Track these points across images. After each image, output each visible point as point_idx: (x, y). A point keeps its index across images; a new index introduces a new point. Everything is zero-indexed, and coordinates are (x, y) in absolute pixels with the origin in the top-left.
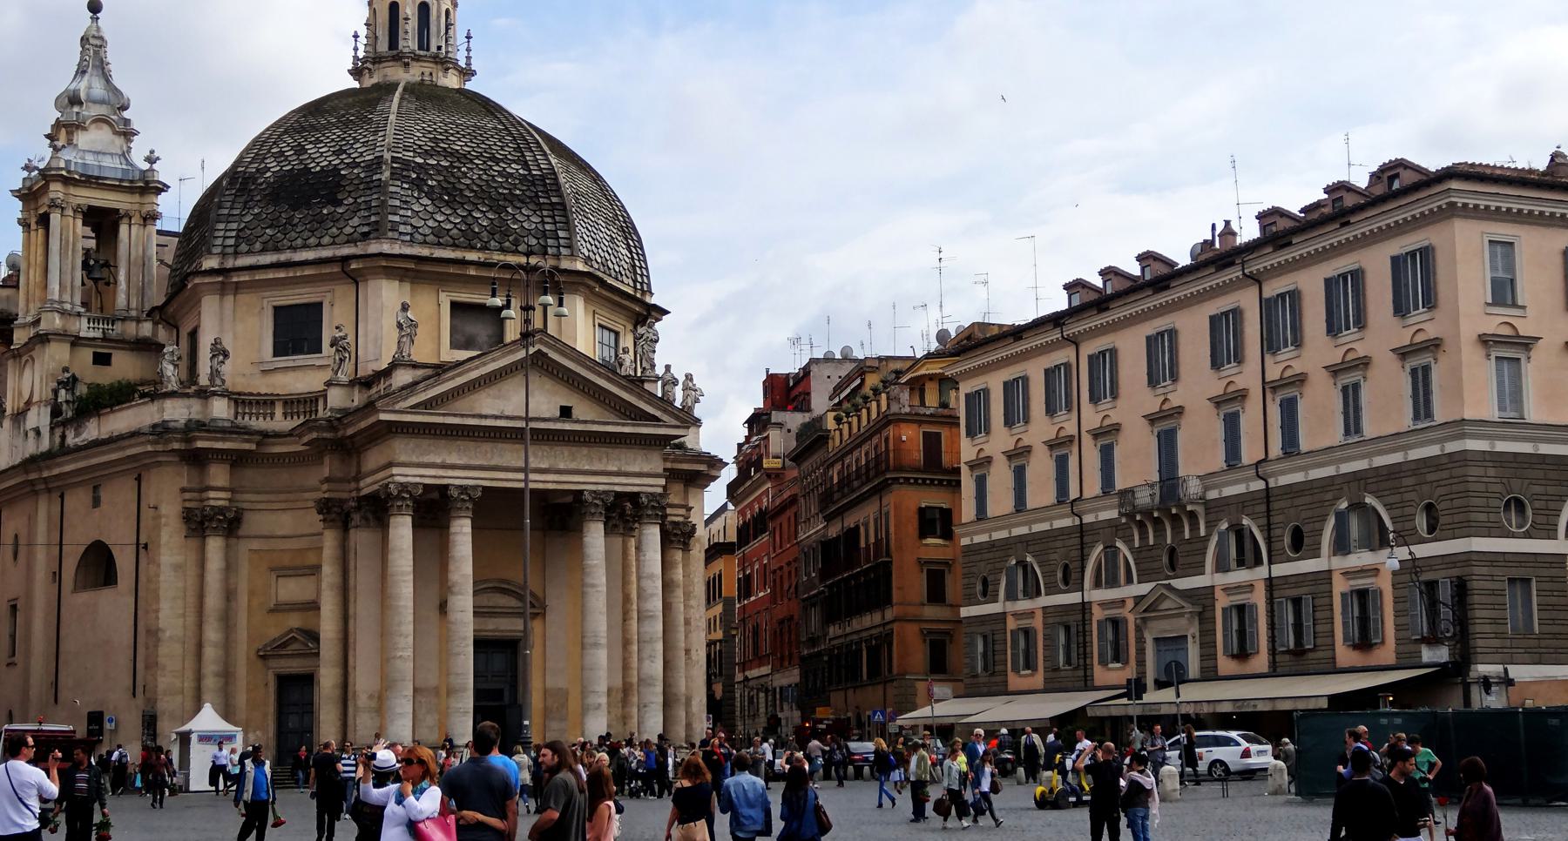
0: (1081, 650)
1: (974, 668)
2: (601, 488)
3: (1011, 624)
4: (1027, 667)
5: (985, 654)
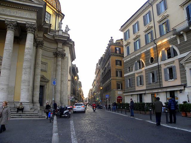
0: (158, 78)
1: (128, 86)
2: (13, 21)
3: (136, 75)
4: (141, 84)
5: (130, 83)
